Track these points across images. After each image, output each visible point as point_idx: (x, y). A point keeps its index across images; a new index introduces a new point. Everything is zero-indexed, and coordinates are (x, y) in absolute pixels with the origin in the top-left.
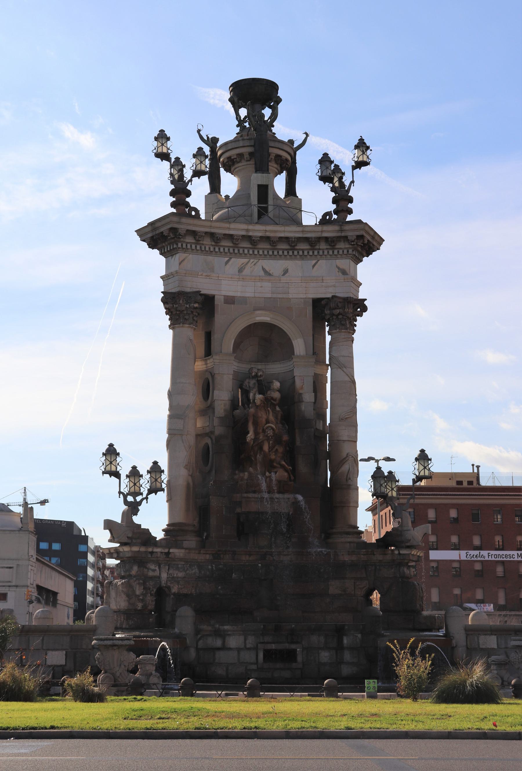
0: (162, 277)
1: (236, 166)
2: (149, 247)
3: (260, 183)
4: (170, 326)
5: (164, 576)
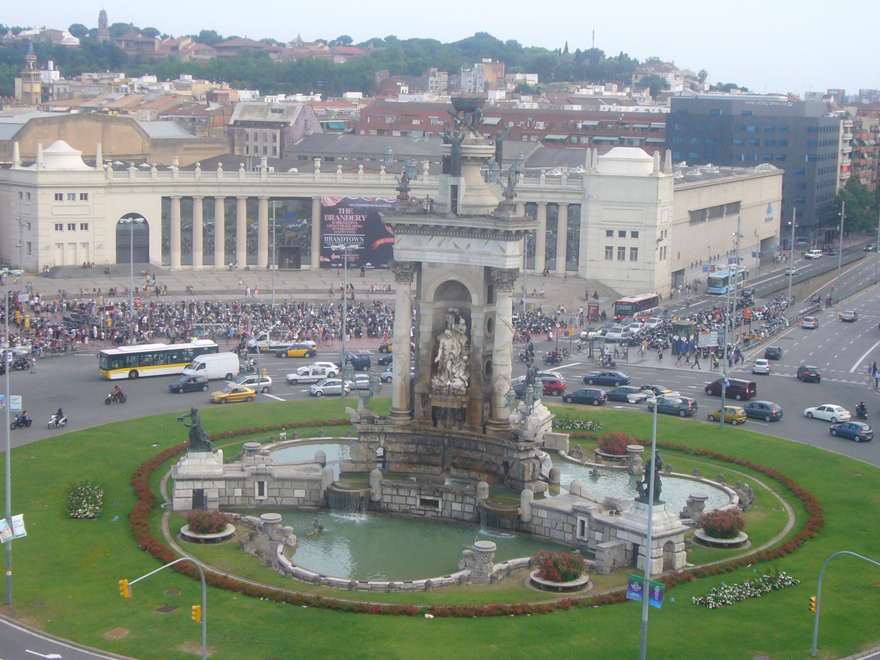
5: (382, 442)
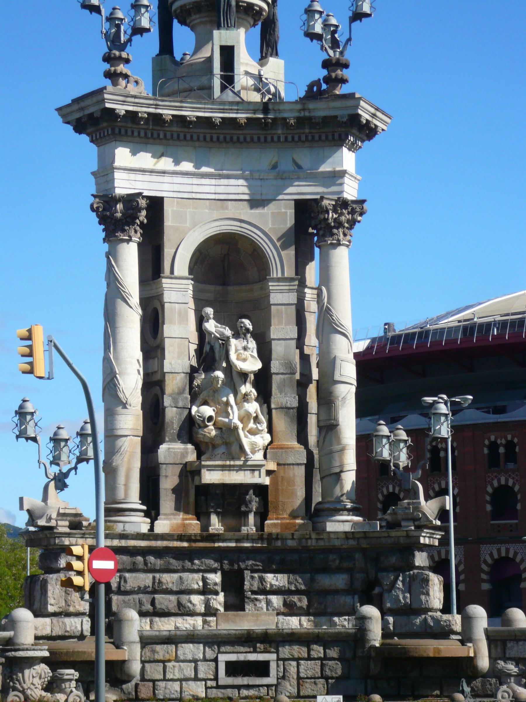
0: (93, 173)
1: (194, 17)
2: (76, 132)
3: (224, 43)
4: (104, 240)
